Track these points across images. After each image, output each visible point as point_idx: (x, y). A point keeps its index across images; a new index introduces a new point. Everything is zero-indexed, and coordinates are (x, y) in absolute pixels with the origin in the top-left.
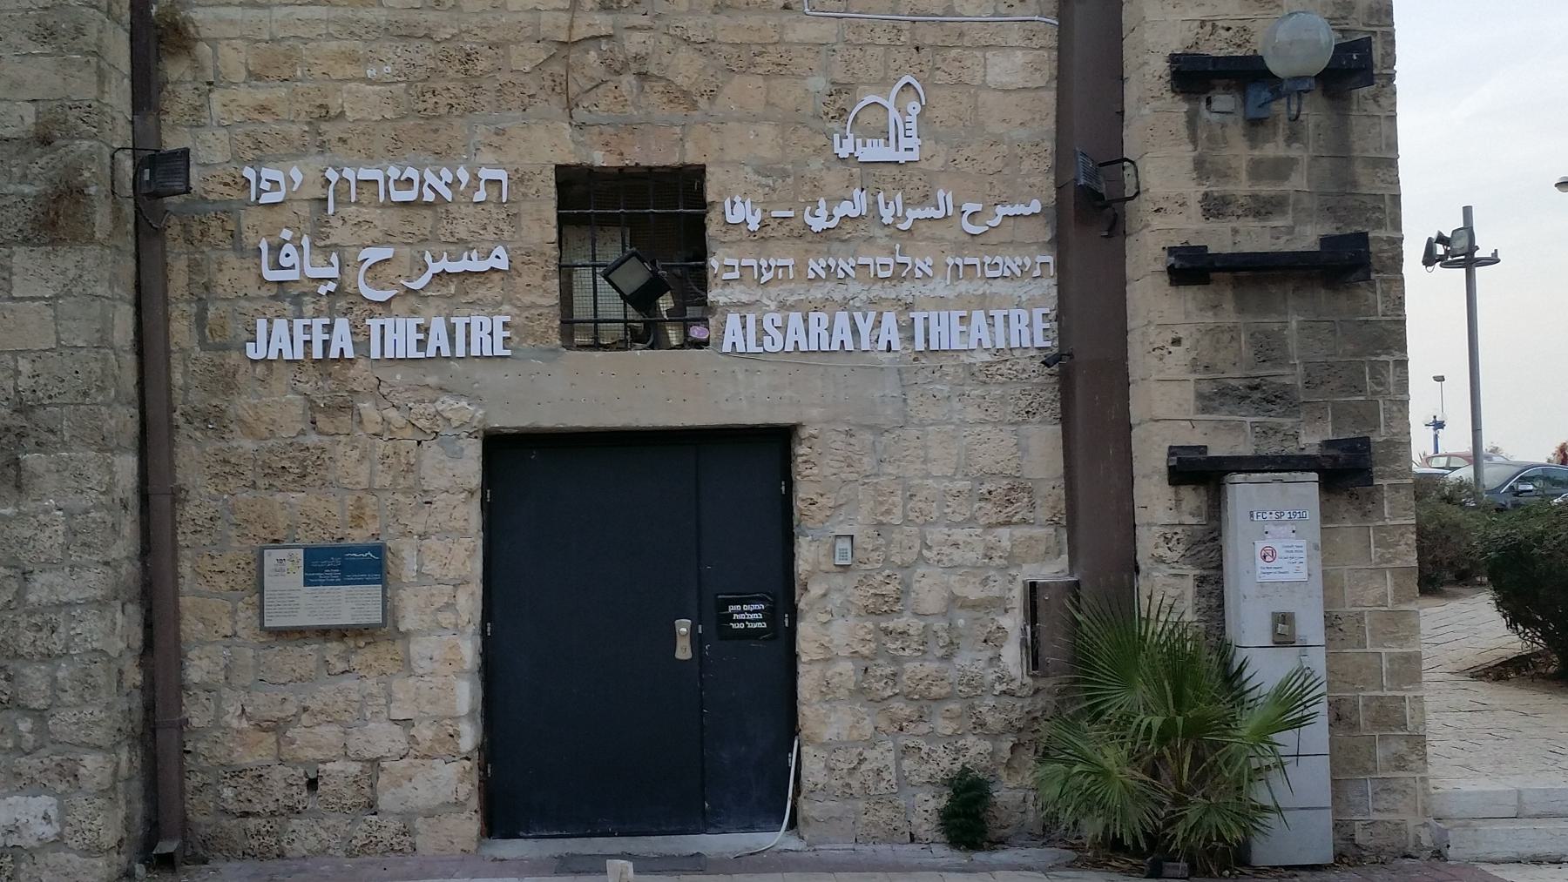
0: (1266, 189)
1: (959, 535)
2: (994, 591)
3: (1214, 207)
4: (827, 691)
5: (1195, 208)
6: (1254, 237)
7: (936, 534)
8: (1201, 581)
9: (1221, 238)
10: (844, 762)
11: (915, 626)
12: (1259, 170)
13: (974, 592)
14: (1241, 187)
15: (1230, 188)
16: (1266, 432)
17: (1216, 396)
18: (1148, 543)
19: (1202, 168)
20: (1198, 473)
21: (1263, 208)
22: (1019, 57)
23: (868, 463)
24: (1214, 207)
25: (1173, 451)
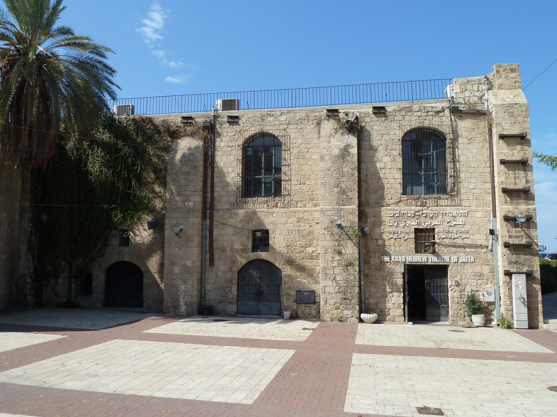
0: (517, 234)
1: (473, 281)
2: (478, 289)
3: (510, 237)
4: (452, 302)
5: (507, 237)
6: (516, 241)
7: (469, 281)
8: (509, 289)
9: (511, 241)
10: (456, 312)
11: (466, 294)
12: (516, 232)
13: (475, 289)
14: (514, 234)
15: (512, 234)
16: (518, 268)
17: (510, 263)
18: (501, 283)
19: (508, 231)
20: (508, 274)
21: (517, 237)
22: (481, 213)
23: (459, 270)
24: (510, 237)
25: (505, 271)
